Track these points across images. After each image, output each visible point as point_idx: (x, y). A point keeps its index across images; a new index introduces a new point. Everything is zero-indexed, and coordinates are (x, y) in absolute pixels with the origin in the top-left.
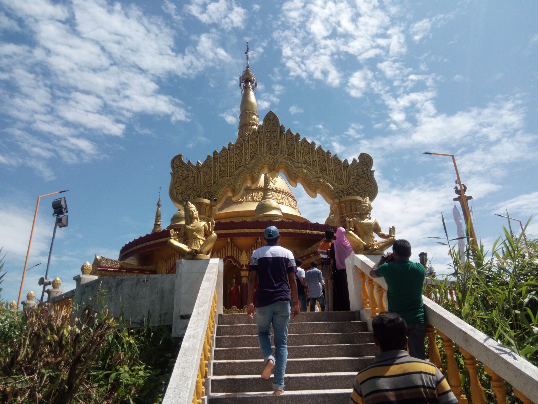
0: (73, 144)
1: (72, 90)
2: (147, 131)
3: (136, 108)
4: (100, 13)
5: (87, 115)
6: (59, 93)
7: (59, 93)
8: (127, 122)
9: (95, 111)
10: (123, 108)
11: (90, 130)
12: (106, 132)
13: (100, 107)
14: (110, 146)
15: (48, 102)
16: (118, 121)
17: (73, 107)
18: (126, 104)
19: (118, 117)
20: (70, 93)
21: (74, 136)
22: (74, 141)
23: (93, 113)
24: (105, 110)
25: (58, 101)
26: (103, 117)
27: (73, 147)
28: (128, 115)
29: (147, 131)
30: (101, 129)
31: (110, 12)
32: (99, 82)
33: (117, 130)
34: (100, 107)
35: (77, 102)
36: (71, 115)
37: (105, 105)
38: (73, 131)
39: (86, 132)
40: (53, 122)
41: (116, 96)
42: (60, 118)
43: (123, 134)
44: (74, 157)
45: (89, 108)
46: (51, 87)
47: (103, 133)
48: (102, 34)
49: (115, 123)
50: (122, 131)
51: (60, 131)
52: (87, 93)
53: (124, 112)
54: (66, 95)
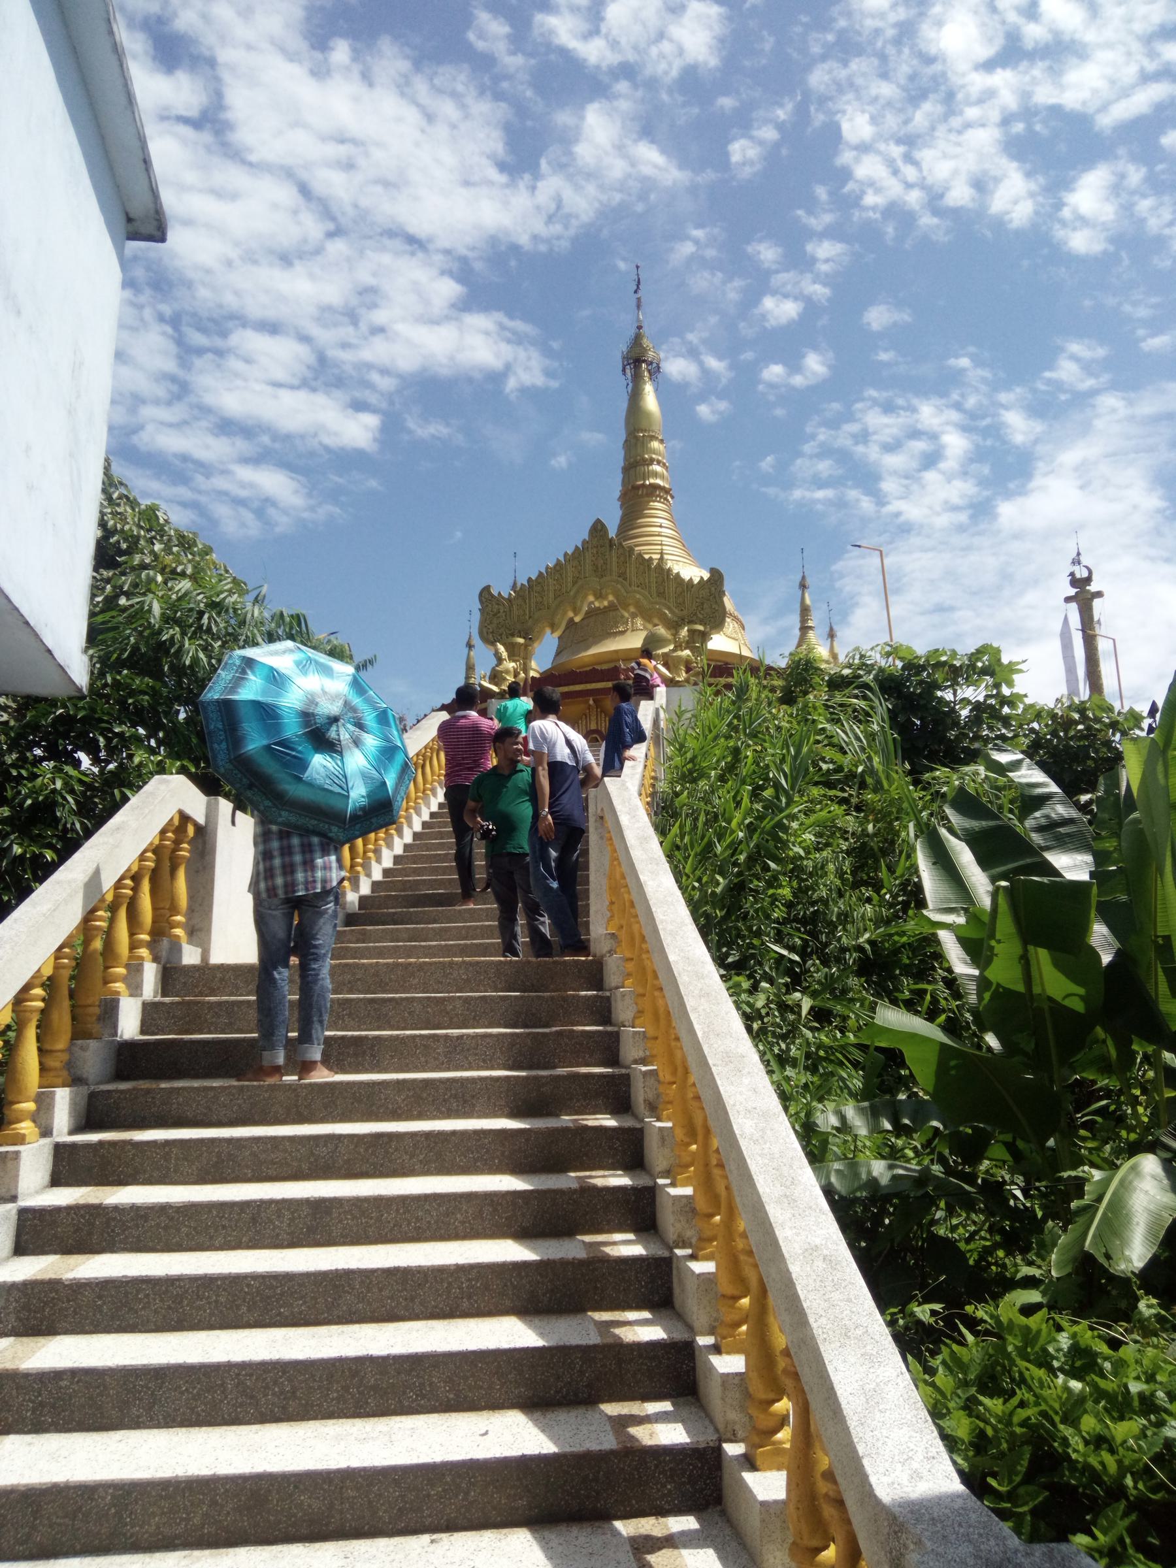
0: (243, 485)
1: (230, 324)
2: (435, 429)
3: (406, 361)
4: (289, 78)
5: (275, 397)
6: (197, 339)
7: (197, 339)
8: (384, 405)
9: (296, 382)
10: (369, 366)
11: (288, 438)
12: (327, 441)
13: (309, 367)
14: (340, 480)
15: (171, 366)
16: (359, 406)
17: (237, 375)
18: (376, 351)
19: (357, 394)
20: (224, 334)
21: (245, 460)
22: (246, 473)
23: (292, 387)
24: (323, 374)
25: (198, 362)
26: (320, 399)
27: (244, 493)
28: (386, 384)
29: (435, 429)
30: (315, 435)
31: (320, 73)
32: (304, 290)
33: (357, 431)
34: (309, 367)
35: (248, 361)
36: (233, 401)
37: (322, 359)
38: (242, 445)
39: (277, 446)
40: (185, 423)
41: (350, 329)
42: (205, 410)
43: (375, 440)
44: (248, 516)
45: (280, 375)
46: (175, 321)
47: (320, 443)
48: (302, 147)
49: (350, 411)
50: (370, 435)
51: (207, 447)
52: (271, 328)
53: (375, 377)
54: (218, 342)
